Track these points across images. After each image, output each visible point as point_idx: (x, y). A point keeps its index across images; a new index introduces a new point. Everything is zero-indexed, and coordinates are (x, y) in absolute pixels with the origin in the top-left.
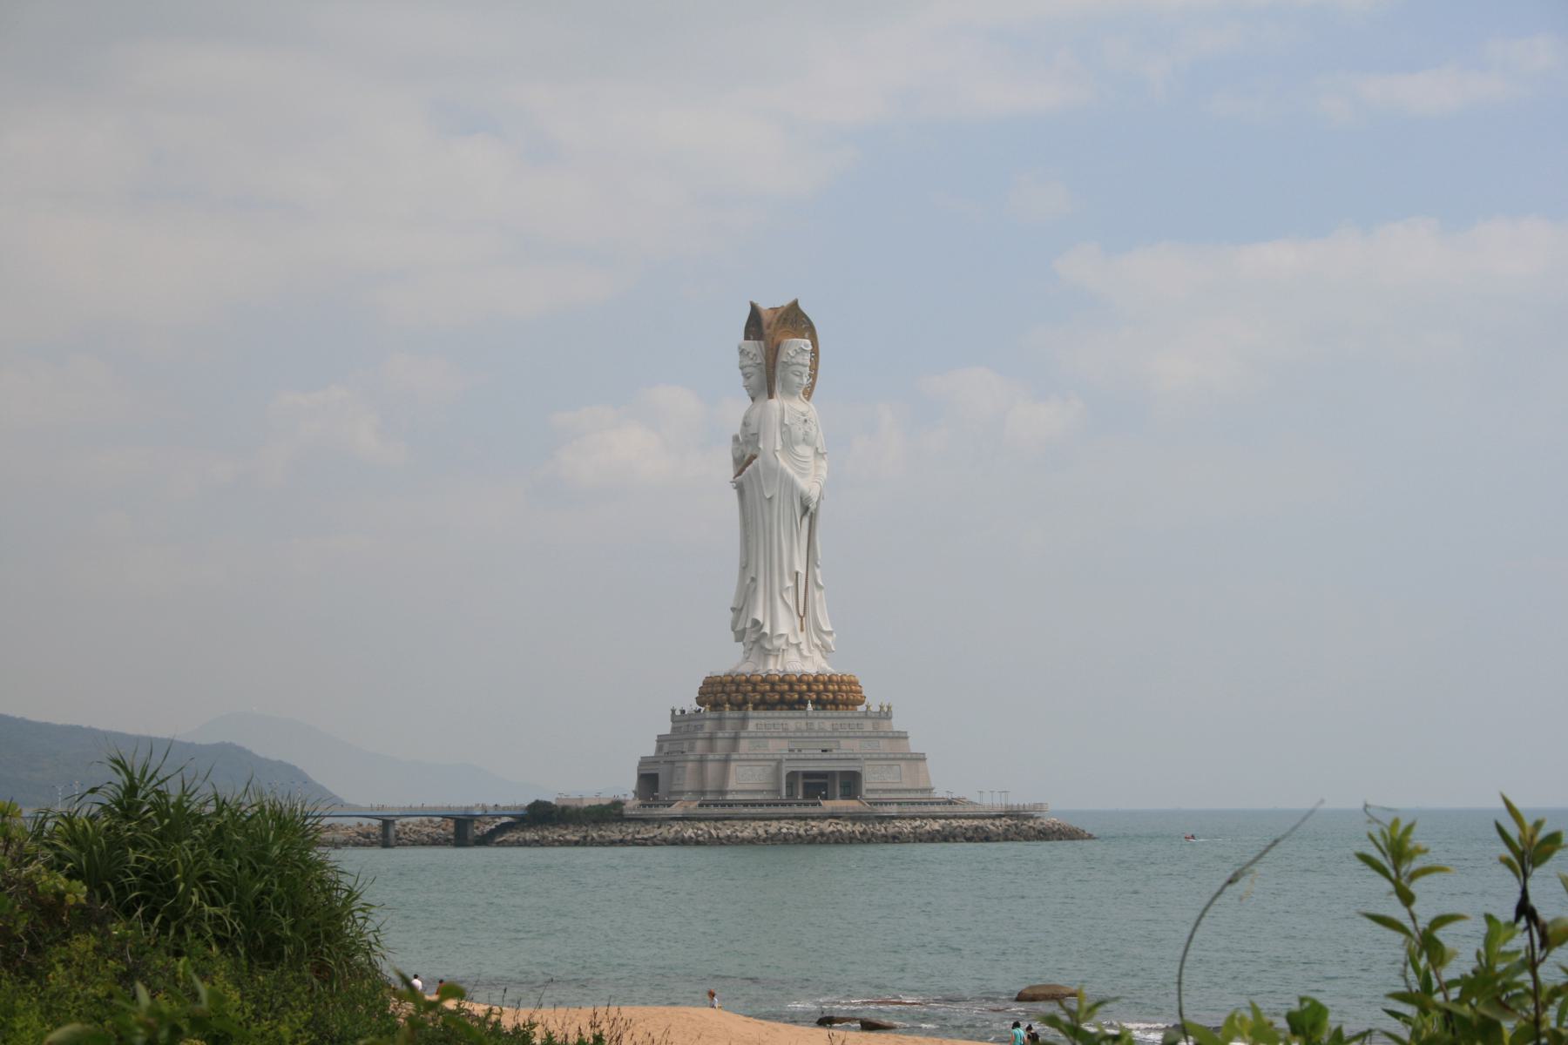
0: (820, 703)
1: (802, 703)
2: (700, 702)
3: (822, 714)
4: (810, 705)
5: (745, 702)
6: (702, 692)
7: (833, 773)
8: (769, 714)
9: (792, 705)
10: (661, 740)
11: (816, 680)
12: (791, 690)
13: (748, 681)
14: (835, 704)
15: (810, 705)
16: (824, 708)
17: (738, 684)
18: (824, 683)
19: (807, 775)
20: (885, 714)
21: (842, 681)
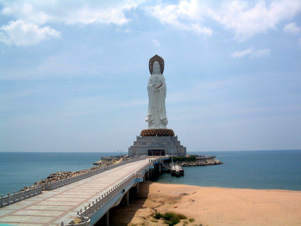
0: (159, 135)
1: (155, 135)
2: (141, 135)
3: (159, 137)
4: (157, 136)
5: (169, 135)
6: (141, 133)
7: (158, 150)
8: (152, 137)
9: (153, 136)
10: (135, 142)
11: (162, 130)
12: (161, 132)
13: (151, 130)
14: (167, 135)
15: (157, 136)
16: (164, 136)
17: (149, 131)
18: (164, 131)
19: (155, 150)
20: (176, 137)
21: (168, 131)
